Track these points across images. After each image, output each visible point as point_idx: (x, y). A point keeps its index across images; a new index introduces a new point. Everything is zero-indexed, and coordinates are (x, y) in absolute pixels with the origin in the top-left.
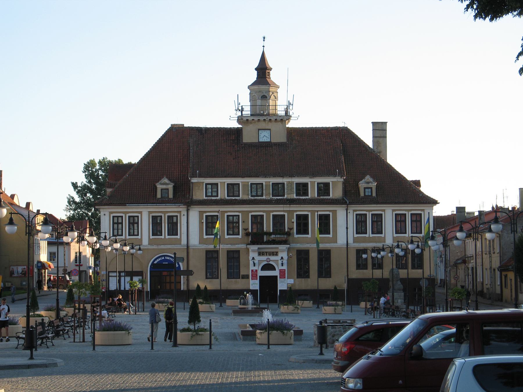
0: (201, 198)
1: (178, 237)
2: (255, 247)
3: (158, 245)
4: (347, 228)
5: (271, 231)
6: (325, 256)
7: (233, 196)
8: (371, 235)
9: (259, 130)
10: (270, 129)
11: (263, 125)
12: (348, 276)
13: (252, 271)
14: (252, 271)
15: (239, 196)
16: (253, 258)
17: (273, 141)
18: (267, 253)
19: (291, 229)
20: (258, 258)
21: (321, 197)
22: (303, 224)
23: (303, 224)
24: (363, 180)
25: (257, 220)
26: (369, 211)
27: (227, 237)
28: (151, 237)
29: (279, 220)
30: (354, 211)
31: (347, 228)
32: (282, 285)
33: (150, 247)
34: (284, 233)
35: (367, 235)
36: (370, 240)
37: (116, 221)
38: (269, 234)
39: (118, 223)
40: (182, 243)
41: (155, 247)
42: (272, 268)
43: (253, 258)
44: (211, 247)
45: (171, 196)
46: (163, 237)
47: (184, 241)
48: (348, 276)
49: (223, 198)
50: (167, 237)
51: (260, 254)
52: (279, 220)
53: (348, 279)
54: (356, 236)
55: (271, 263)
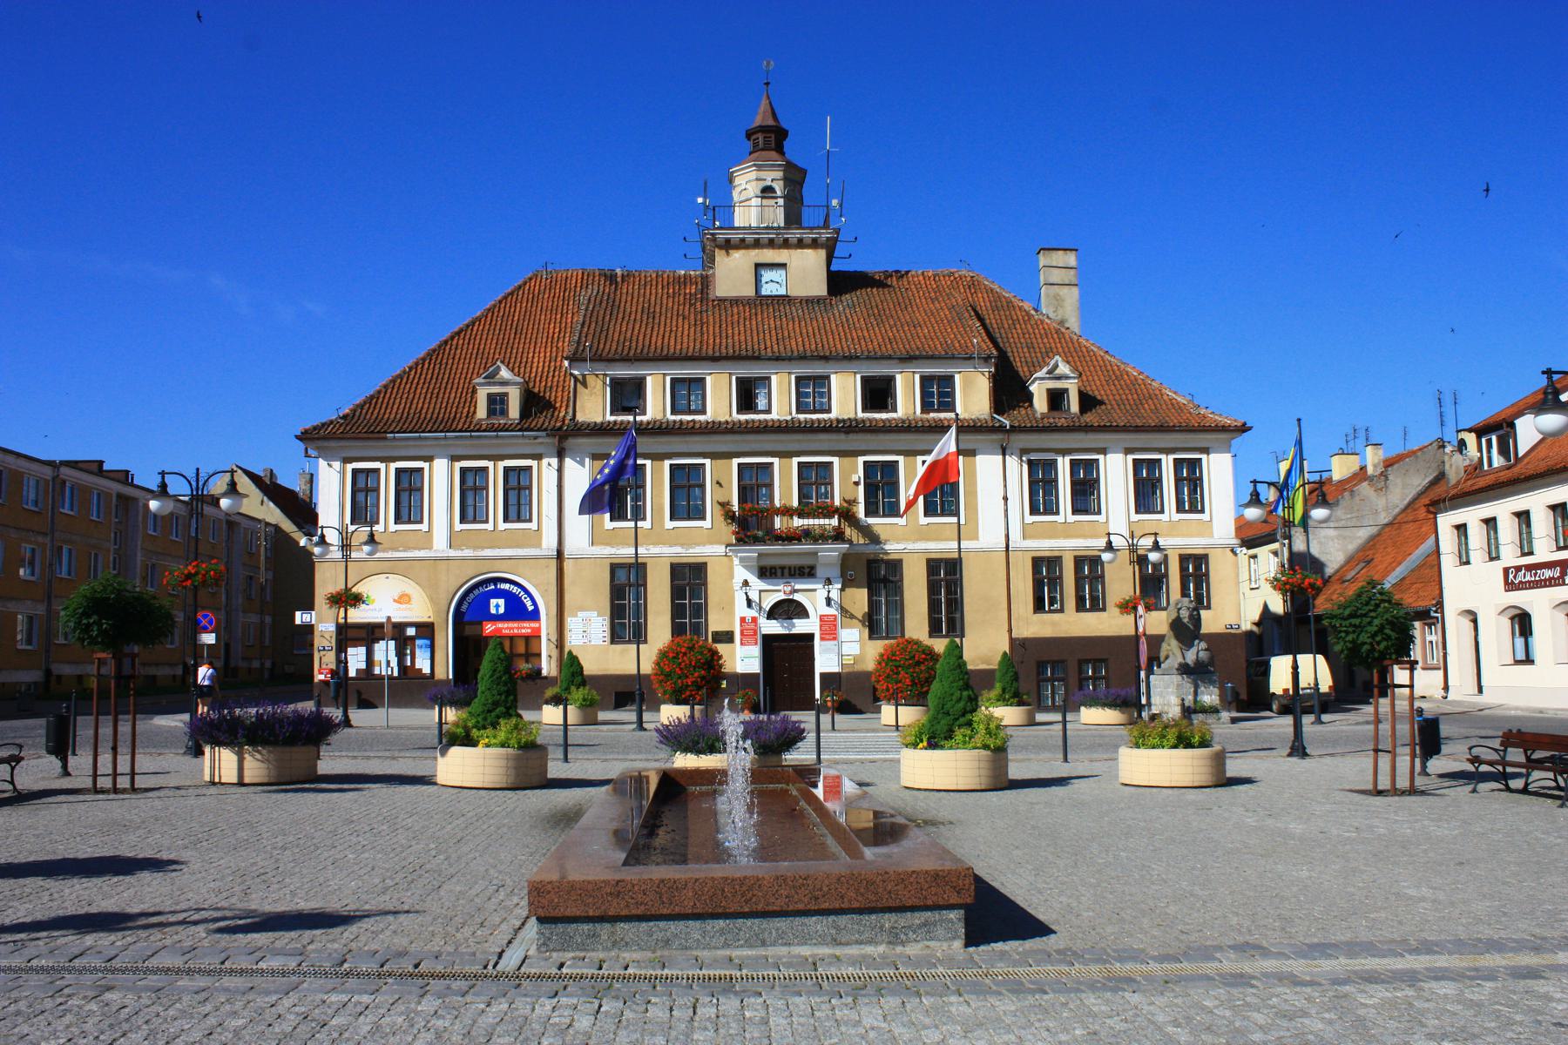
0: (599, 420)
1: (533, 526)
2: (752, 552)
3: (475, 548)
4: (1006, 499)
5: (795, 504)
6: (946, 577)
7: (690, 412)
8: (1072, 518)
9: (758, 266)
10: (783, 266)
11: (769, 255)
12: (1010, 631)
13: (743, 620)
14: (743, 620)
15: (703, 412)
16: (746, 583)
17: (793, 293)
18: (783, 568)
19: (854, 502)
20: (757, 584)
21: (932, 415)
22: (881, 486)
23: (881, 486)
24: (1045, 370)
25: (754, 482)
26: (1064, 452)
27: (669, 524)
28: (458, 526)
29: (814, 478)
30: (1023, 452)
31: (1006, 499)
32: (825, 661)
33: (452, 553)
34: (828, 512)
35: (1060, 519)
36: (1067, 530)
37: (361, 484)
38: (787, 512)
39: (367, 490)
40: (544, 545)
41: (468, 553)
42: (801, 612)
43: (746, 583)
44: (626, 552)
45: (514, 411)
46: (490, 526)
47: (549, 542)
48: (1010, 631)
49: (659, 417)
50: (502, 526)
51: (765, 573)
52: (814, 478)
53: (1011, 638)
54: (1030, 519)
55: (797, 597)
